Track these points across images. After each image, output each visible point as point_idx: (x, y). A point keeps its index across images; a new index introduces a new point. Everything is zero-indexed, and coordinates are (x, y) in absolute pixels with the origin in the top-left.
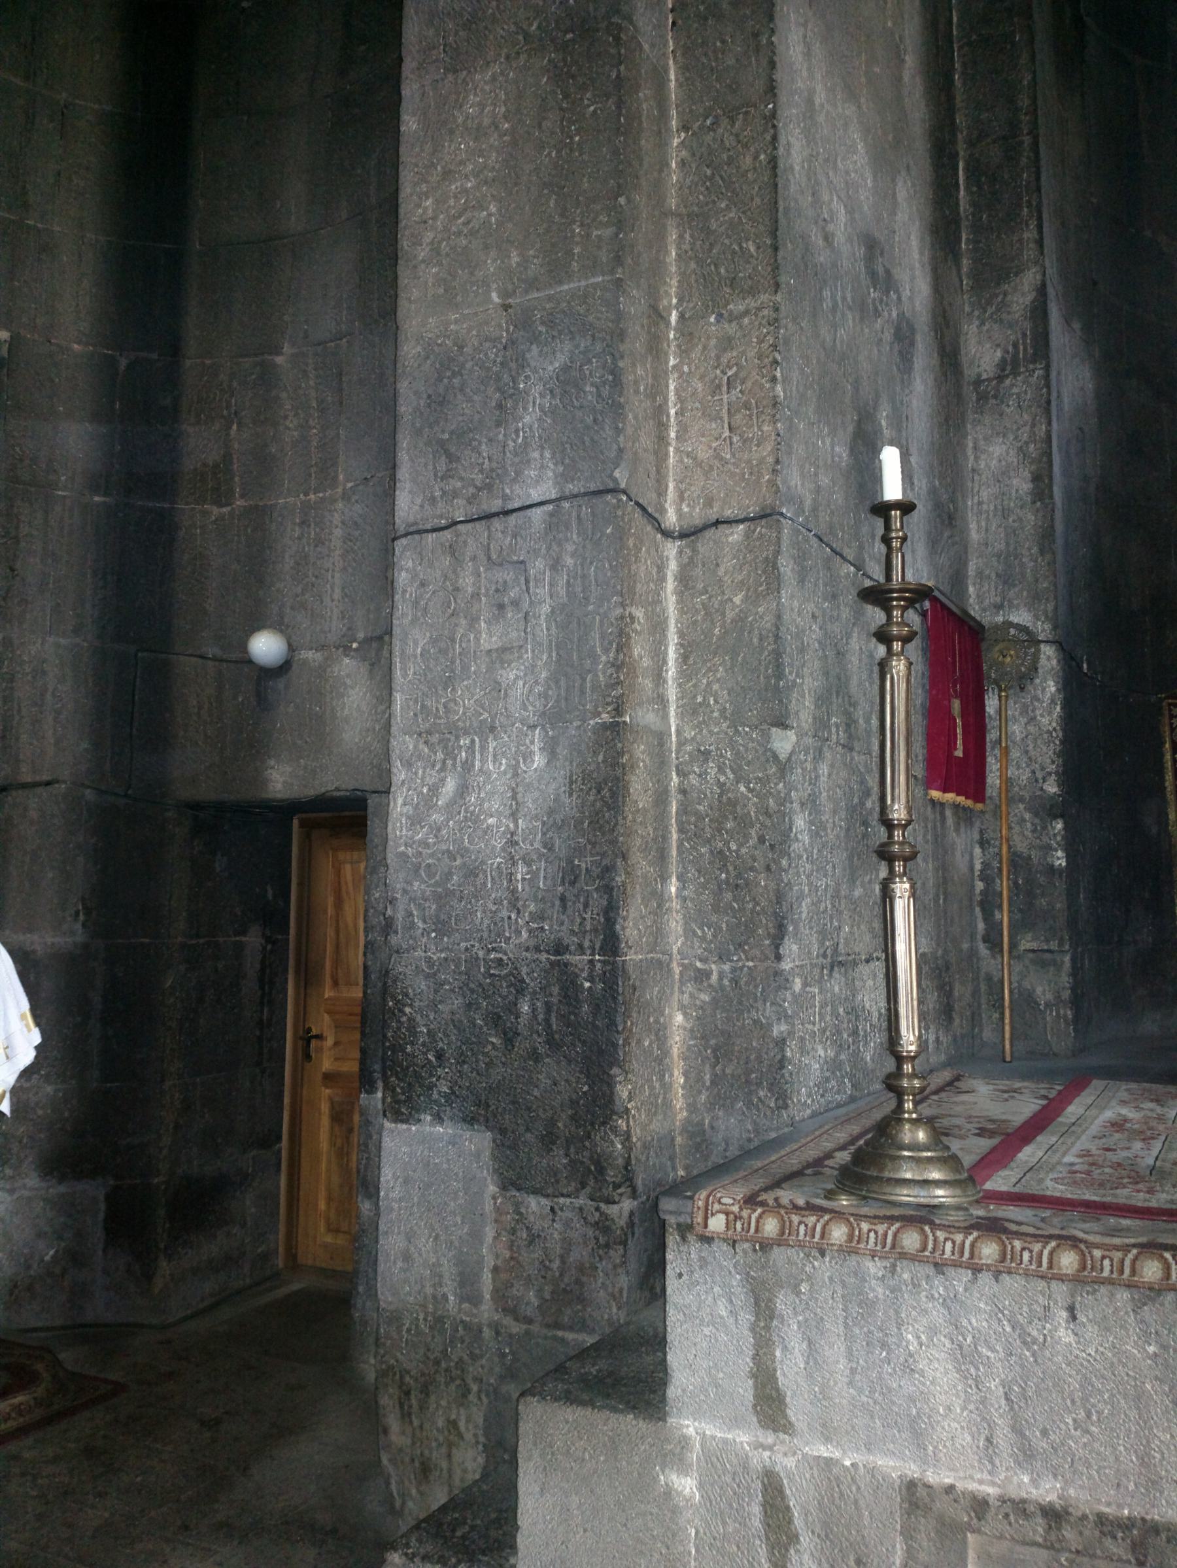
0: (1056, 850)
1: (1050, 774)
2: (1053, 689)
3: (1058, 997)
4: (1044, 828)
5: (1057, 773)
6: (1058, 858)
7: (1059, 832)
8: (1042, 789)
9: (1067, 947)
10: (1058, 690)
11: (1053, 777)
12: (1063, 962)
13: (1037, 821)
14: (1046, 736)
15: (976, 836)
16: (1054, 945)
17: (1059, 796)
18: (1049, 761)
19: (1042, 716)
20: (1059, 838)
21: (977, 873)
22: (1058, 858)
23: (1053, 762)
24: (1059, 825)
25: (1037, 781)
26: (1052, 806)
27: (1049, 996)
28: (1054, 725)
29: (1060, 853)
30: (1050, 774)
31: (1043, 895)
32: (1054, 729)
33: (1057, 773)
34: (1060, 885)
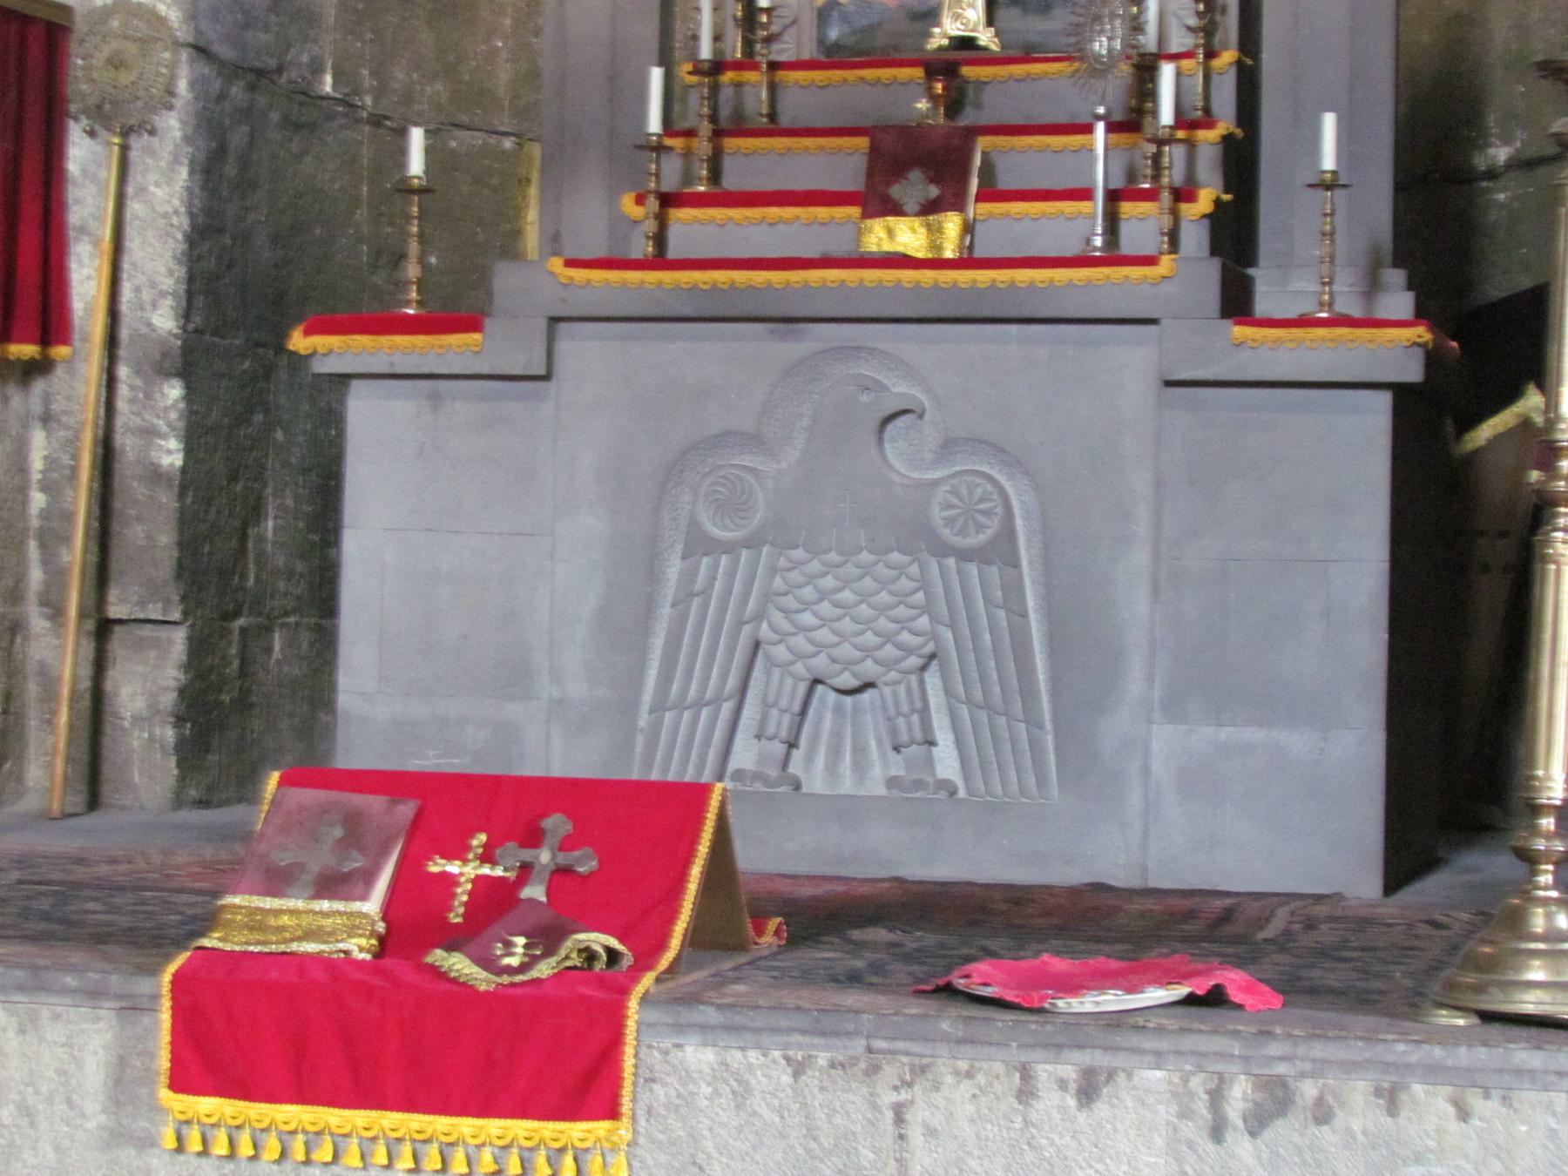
0: (164, 437)
1: (163, 294)
2: (178, 134)
3: (153, 706)
4: (148, 396)
5: (174, 294)
6: (169, 452)
7: (173, 406)
8: (149, 324)
9: (176, 615)
10: (187, 139)
11: (169, 301)
12: (170, 642)
13: (138, 382)
14: (162, 222)
15: (36, 406)
16: (154, 612)
17: (175, 336)
18: (163, 270)
19: (157, 185)
20: (173, 415)
21: (36, 477)
22: (169, 452)
23: (171, 273)
24: (174, 391)
25: (142, 308)
26: (164, 355)
27: (139, 704)
28: (176, 202)
29: (173, 444)
30: (163, 294)
31: (139, 519)
32: (176, 212)
33: (174, 294)
34: (167, 500)
